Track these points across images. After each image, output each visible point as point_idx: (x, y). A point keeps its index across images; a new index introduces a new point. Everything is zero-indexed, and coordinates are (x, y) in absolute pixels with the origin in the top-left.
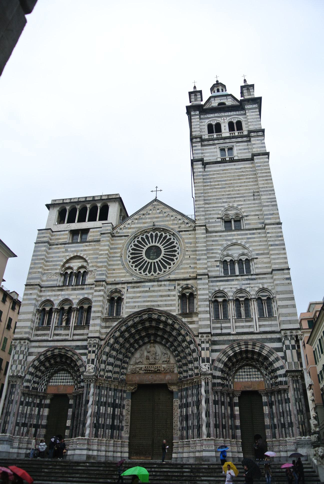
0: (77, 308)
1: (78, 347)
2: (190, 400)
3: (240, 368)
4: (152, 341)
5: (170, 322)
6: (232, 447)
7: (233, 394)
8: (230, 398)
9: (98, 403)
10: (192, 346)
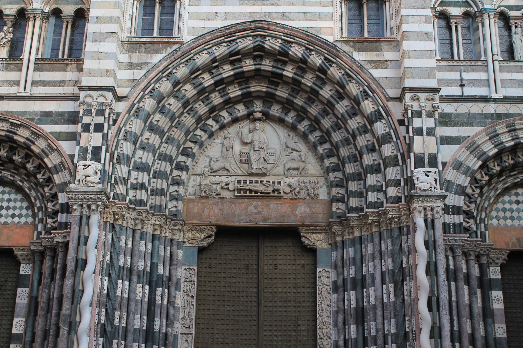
0: (43, 12)
1: (47, 116)
2: (369, 268)
3: (506, 191)
4: (258, 115)
5: (316, 60)
7: (488, 255)
8: (481, 267)
9: (110, 270)
10: (380, 128)
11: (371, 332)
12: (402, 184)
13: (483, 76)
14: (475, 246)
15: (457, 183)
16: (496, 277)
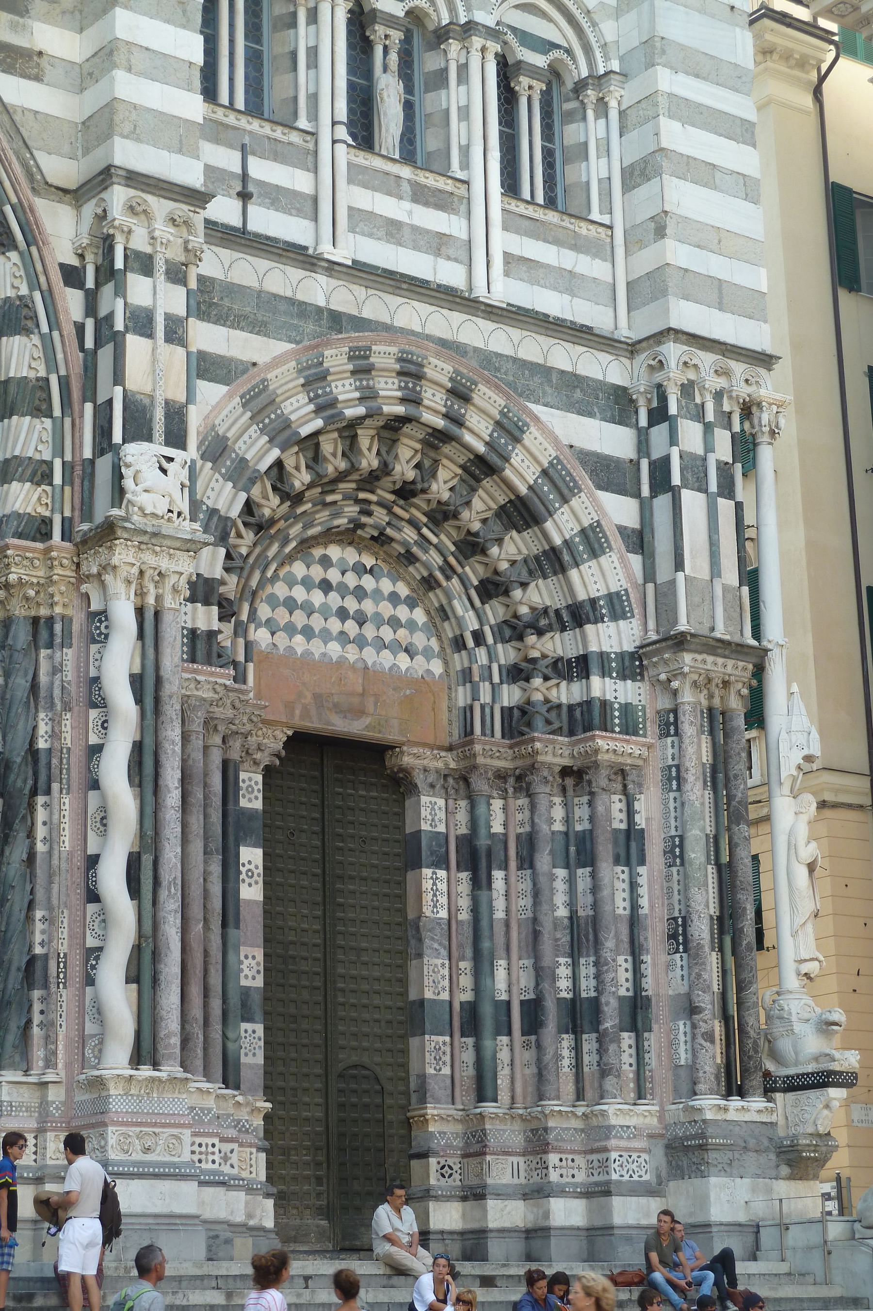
12: (58, 479)
13: (299, 180)
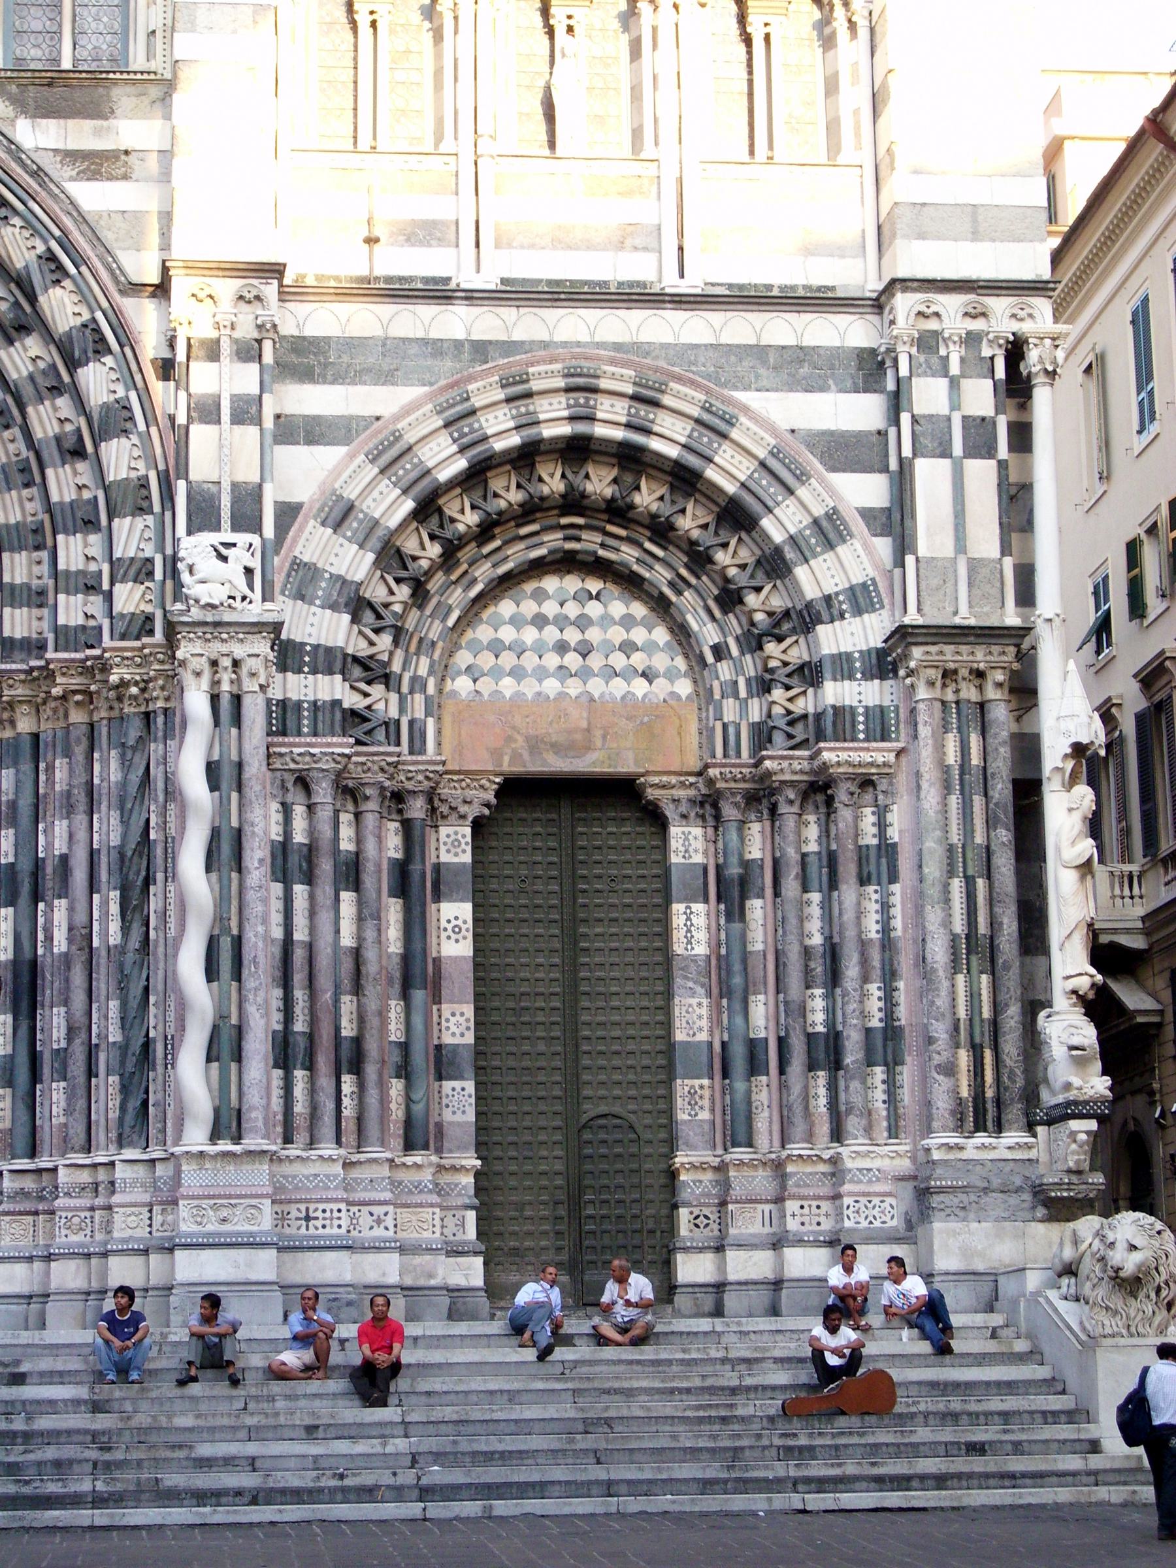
2: (56, 837)
3: (506, 583)
6: (404, 1215)
7: (431, 796)
10: (98, 381)
11: (55, 1038)
14: (382, 770)
15: (333, 570)
16: (456, 860)
